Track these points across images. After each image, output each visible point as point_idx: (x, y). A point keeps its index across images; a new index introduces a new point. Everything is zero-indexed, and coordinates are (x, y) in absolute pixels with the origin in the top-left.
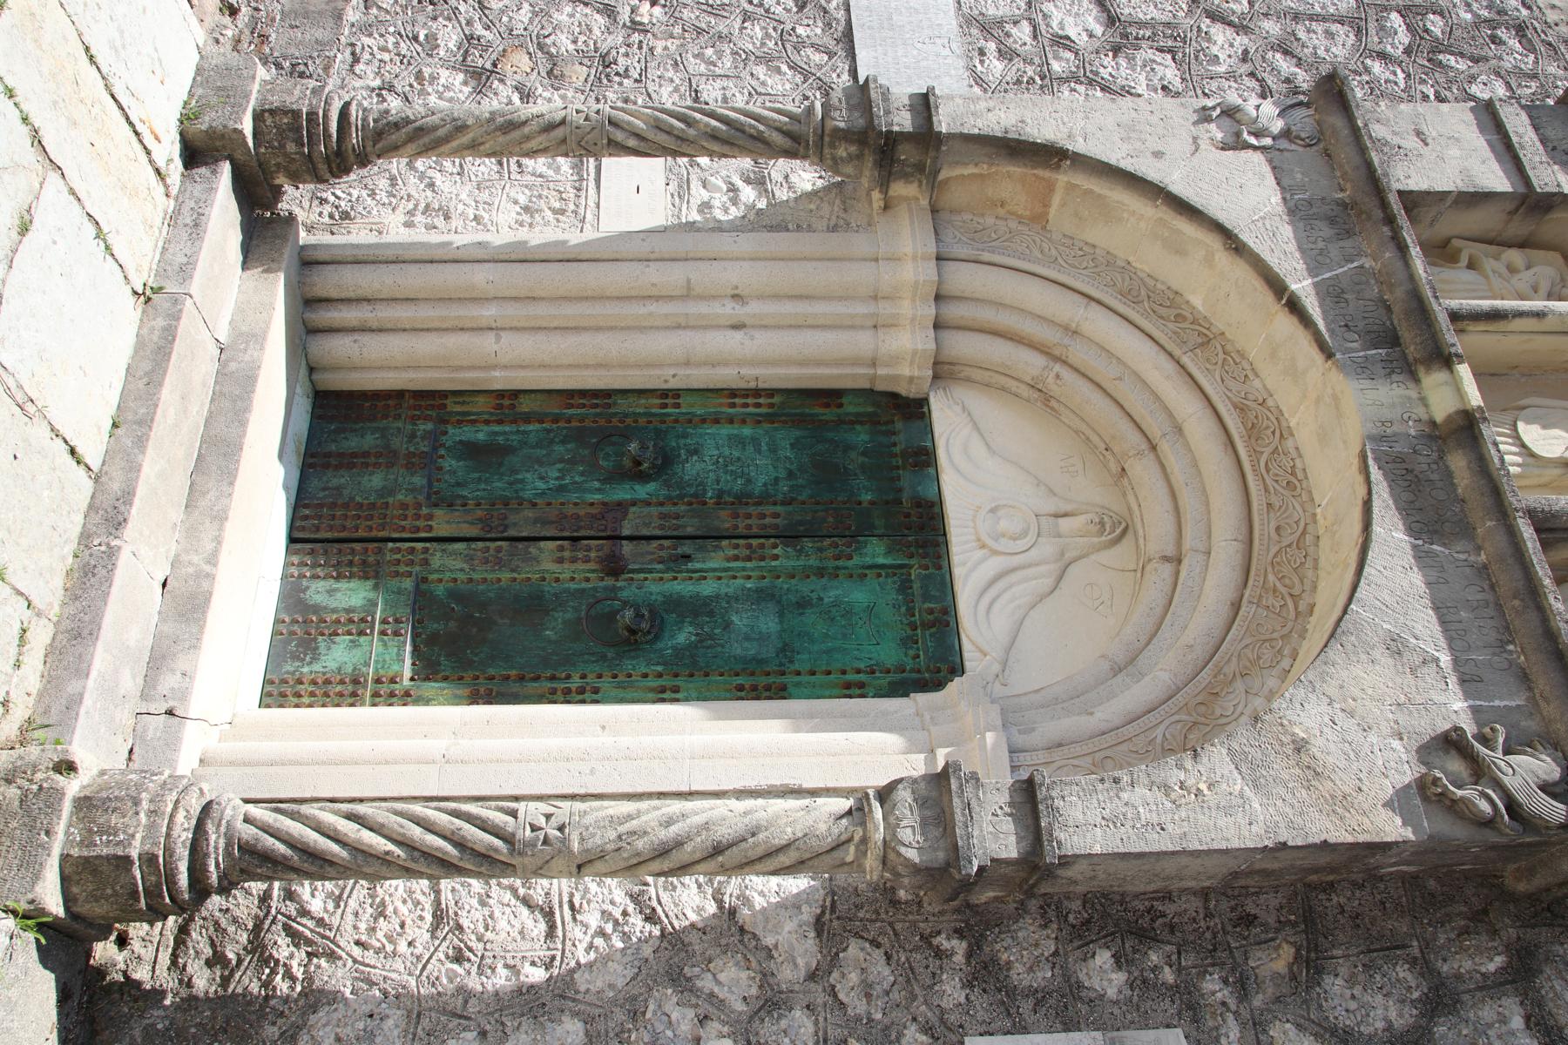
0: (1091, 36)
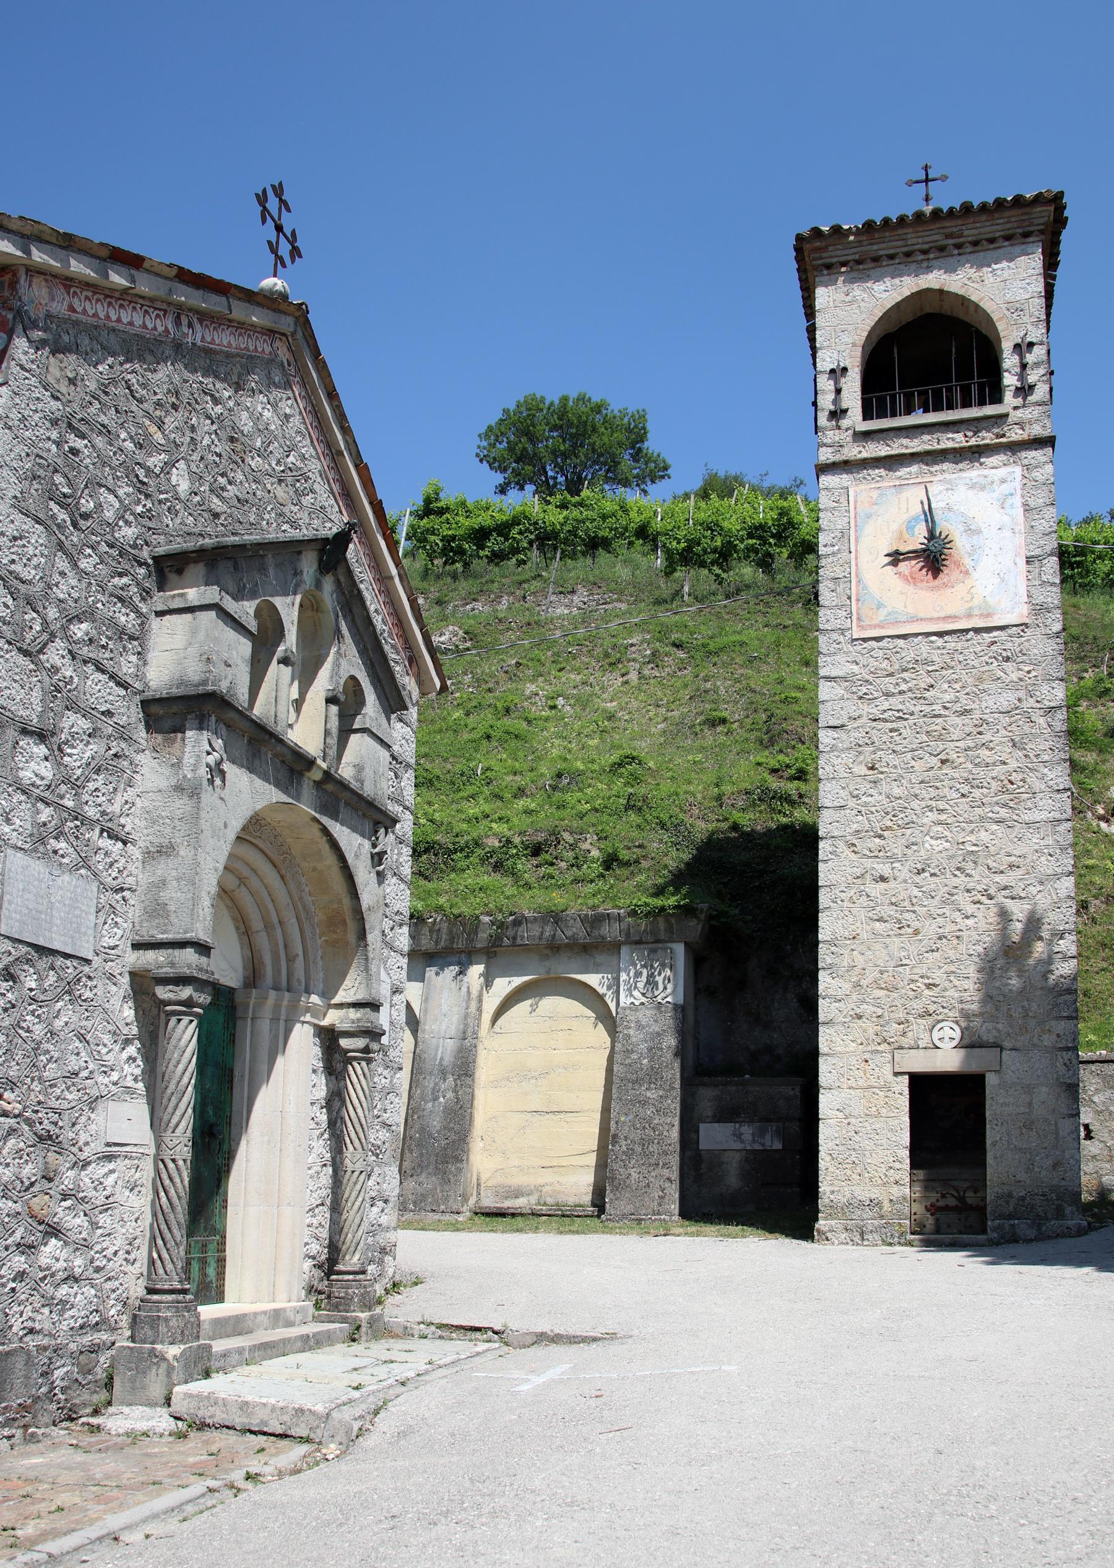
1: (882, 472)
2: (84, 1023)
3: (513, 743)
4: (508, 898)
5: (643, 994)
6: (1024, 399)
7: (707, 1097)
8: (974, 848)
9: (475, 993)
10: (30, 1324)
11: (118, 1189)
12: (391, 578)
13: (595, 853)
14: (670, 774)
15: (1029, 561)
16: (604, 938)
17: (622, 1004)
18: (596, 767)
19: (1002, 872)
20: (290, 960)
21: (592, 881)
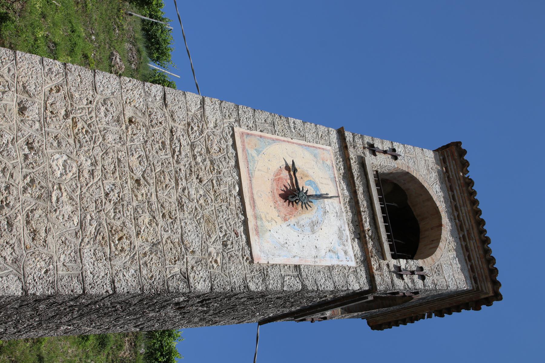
1: (342, 171)
6: (394, 272)
8: (54, 199)
15: (297, 267)
19: (28, 222)
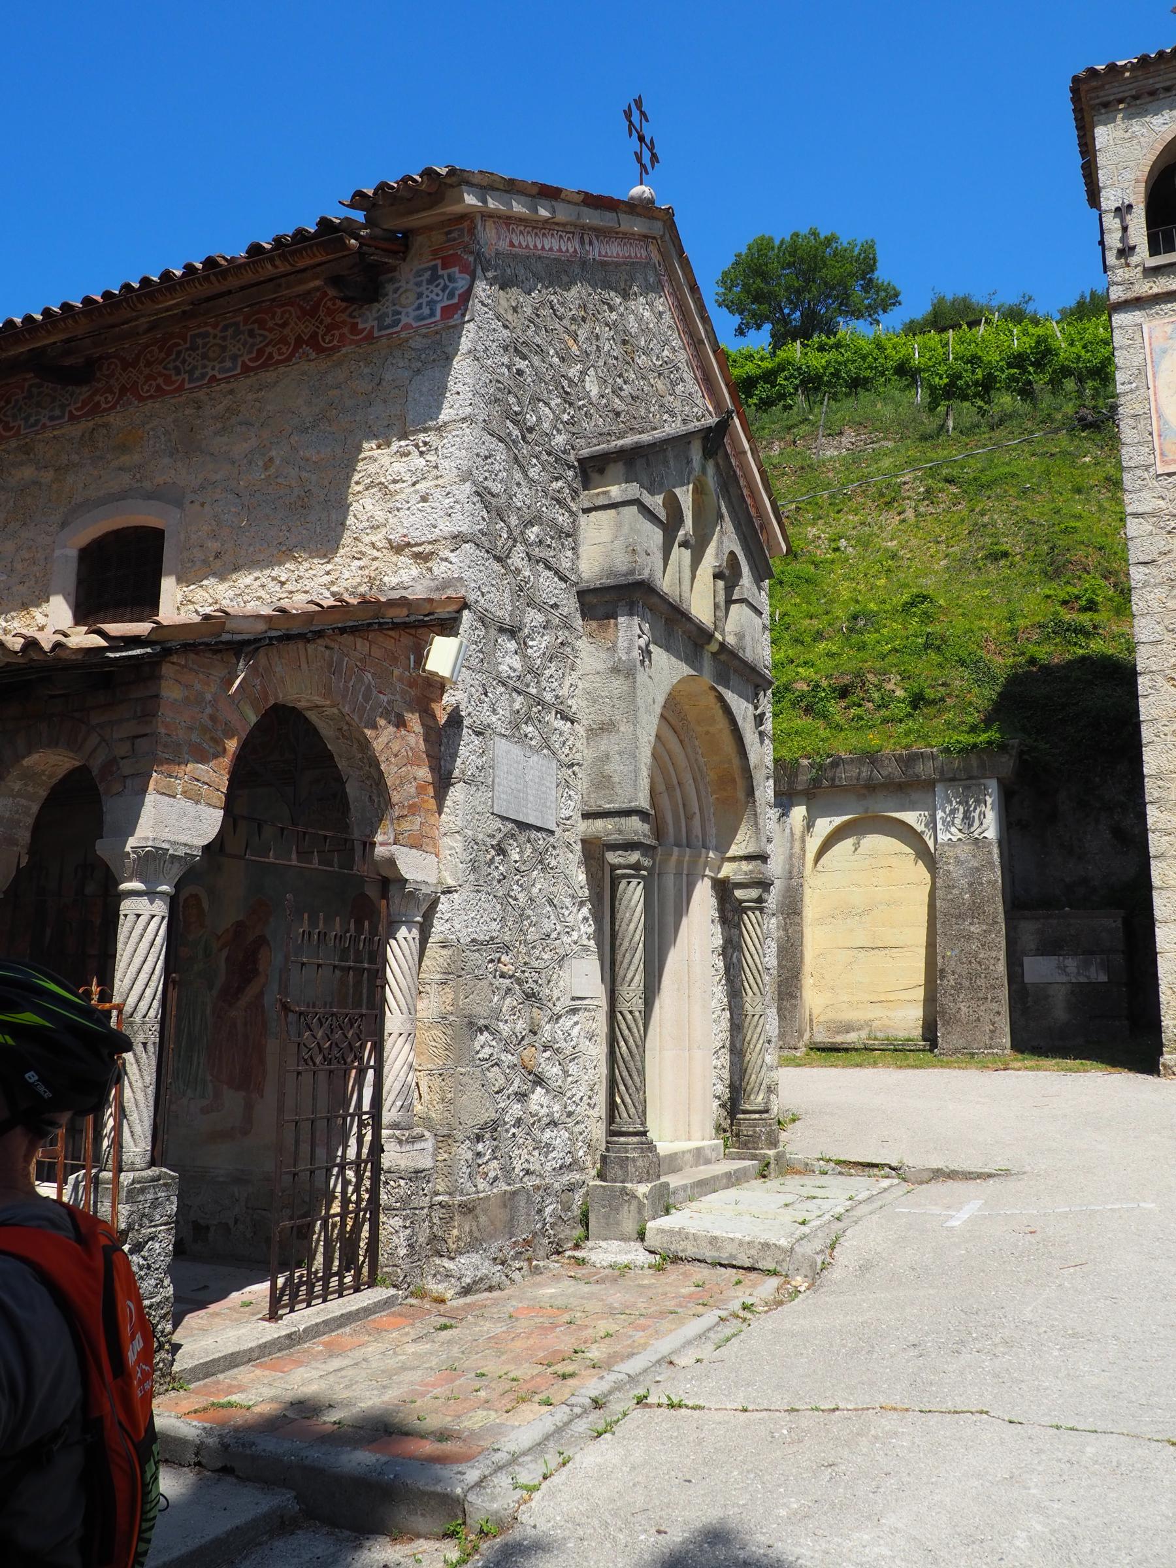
0: (516, 653)
2: (553, 889)
3: (805, 587)
4: (822, 740)
5: (960, 830)
7: (1029, 929)
9: (798, 832)
10: (526, 1166)
11: (582, 1039)
12: (745, 453)
13: (900, 693)
14: (960, 611)
16: (918, 776)
17: (939, 841)
18: (888, 607)
20: (689, 818)
21: (901, 721)
